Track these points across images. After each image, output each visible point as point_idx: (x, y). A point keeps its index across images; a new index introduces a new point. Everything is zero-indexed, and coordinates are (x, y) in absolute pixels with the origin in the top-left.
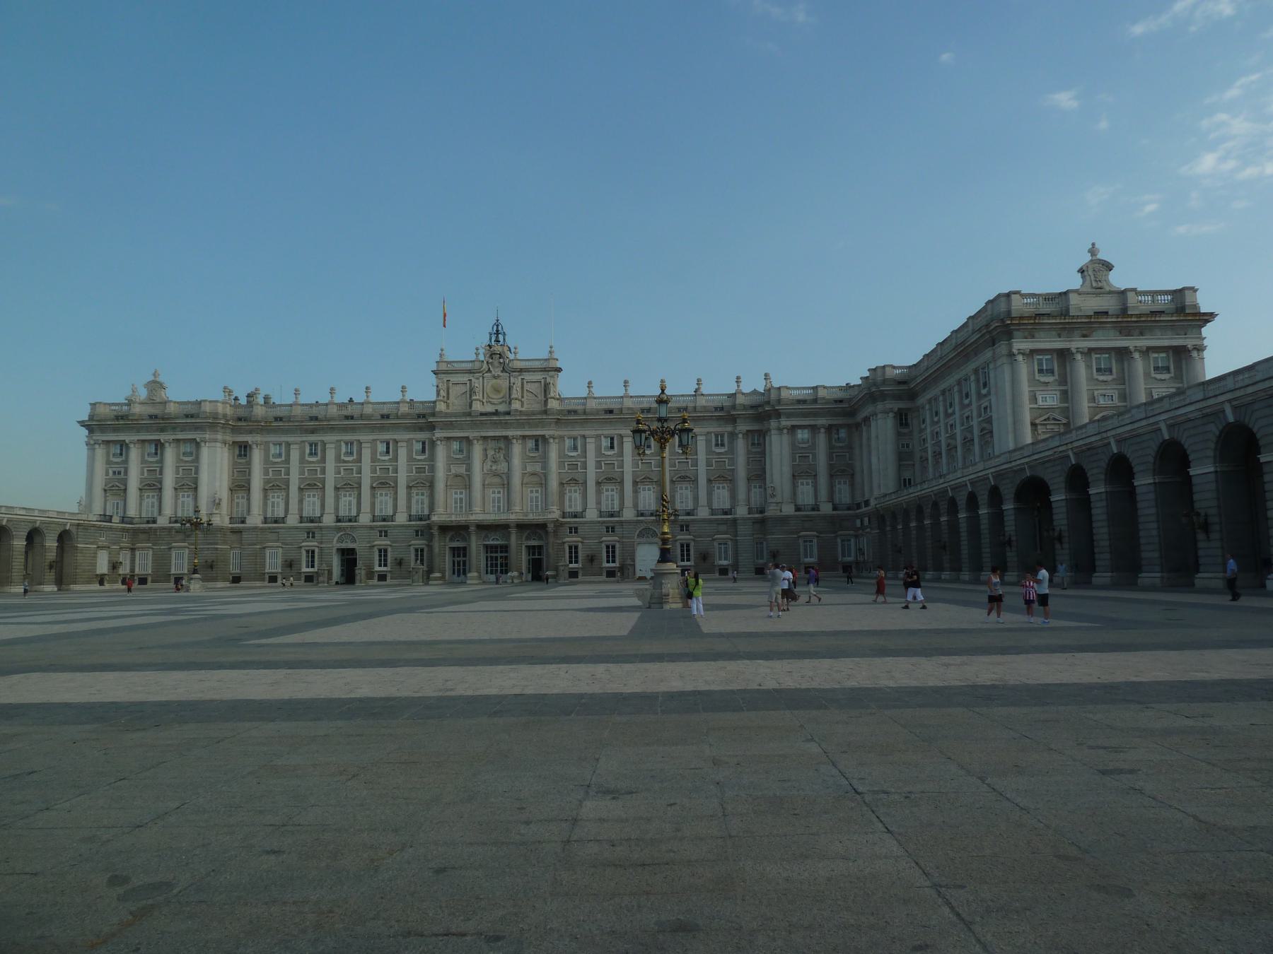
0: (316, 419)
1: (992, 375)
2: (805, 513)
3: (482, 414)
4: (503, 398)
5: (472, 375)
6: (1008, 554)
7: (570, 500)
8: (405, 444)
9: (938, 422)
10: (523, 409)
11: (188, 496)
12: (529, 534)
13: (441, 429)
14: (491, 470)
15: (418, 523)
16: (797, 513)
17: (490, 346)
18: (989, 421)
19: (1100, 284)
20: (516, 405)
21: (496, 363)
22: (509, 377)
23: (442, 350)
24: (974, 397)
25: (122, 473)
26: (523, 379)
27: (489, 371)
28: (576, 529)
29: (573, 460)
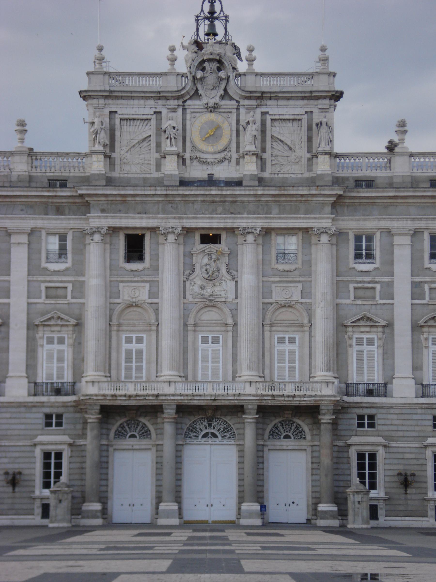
3: (184, 183)
4: (223, 151)
5: (160, 102)
7: (360, 360)
10: (266, 175)
12: (276, 427)
13: (103, 211)
14: (203, 297)
15: (53, 399)
17: (199, 45)
21: (211, 79)
22: (238, 109)
23: (100, 49)
26: (264, 114)
27: (196, 95)
28: (371, 417)
29: (367, 279)
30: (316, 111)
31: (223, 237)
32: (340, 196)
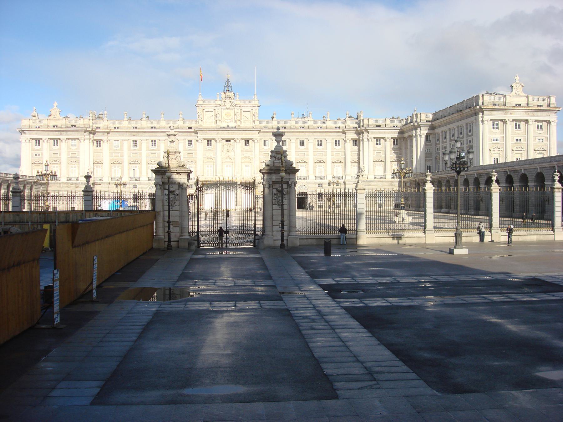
0: (136, 128)
1: (474, 127)
2: (378, 179)
3: (221, 128)
6: (481, 204)
8: (182, 141)
9: (446, 142)
10: (241, 125)
11: (75, 167)
13: (201, 135)
16: (375, 179)
18: (472, 147)
19: (519, 93)
20: (238, 123)
24: (465, 136)
25: (40, 155)
30: (253, 109)
31: (231, 141)
32: (260, 131)
